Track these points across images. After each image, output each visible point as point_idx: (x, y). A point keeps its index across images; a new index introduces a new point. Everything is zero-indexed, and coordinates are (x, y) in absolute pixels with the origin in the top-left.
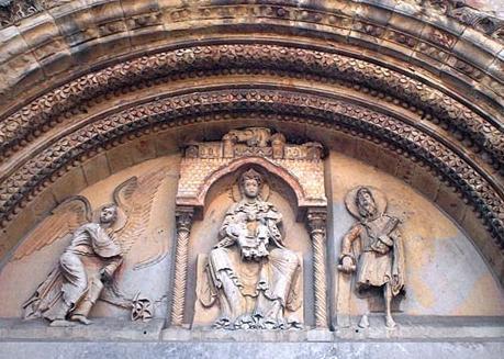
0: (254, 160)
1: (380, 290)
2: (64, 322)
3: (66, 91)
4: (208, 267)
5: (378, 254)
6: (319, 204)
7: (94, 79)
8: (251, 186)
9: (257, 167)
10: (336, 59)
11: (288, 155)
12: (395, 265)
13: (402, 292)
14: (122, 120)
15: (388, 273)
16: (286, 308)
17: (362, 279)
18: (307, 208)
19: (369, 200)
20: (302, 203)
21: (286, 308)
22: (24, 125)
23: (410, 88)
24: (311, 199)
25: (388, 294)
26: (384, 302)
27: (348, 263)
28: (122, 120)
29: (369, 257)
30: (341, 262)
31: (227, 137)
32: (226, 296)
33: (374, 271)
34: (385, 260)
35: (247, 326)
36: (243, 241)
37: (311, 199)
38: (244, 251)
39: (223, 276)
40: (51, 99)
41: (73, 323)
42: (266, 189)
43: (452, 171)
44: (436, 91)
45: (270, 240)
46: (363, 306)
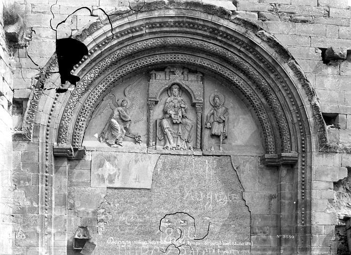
0: (175, 82)
1: (218, 137)
2: (116, 145)
3: (110, 59)
4: (161, 126)
5: (219, 123)
6: (200, 102)
7: (120, 55)
8: (175, 90)
9: (178, 84)
10: (211, 47)
11: (190, 79)
12: (225, 129)
13: (226, 137)
14: (129, 68)
15: (222, 131)
16: (187, 142)
17: (213, 133)
18: (195, 103)
19: (218, 101)
20: (194, 101)
21: (187, 142)
22: (97, 75)
23: (238, 62)
24: (197, 100)
25: (221, 138)
26: (220, 140)
27: (209, 125)
28: (129, 68)
29: (216, 123)
30: (206, 125)
31: (166, 70)
32: (167, 137)
33: (217, 129)
34: (222, 125)
35: (174, 149)
36: (173, 116)
37: (197, 100)
38: (174, 121)
39: (167, 130)
40: (105, 63)
41: (118, 145)
42: (181, 91)
43: (248, 96)
44: (247, 64)
45: (182, 116)
46: (213, 141)
